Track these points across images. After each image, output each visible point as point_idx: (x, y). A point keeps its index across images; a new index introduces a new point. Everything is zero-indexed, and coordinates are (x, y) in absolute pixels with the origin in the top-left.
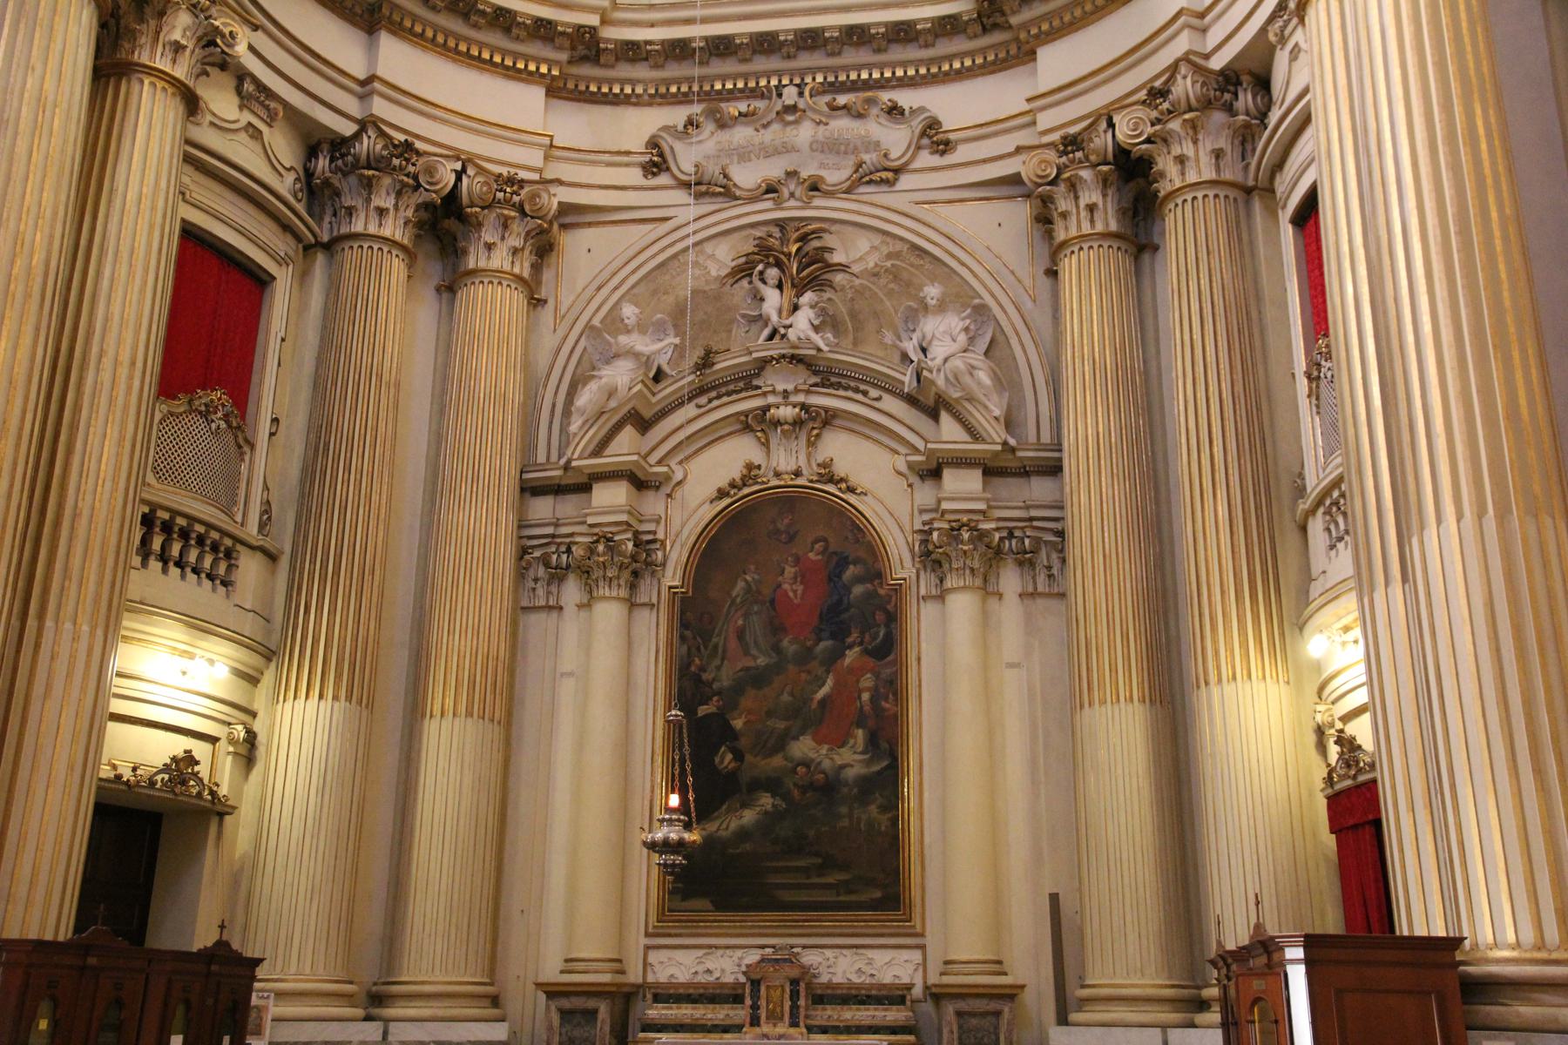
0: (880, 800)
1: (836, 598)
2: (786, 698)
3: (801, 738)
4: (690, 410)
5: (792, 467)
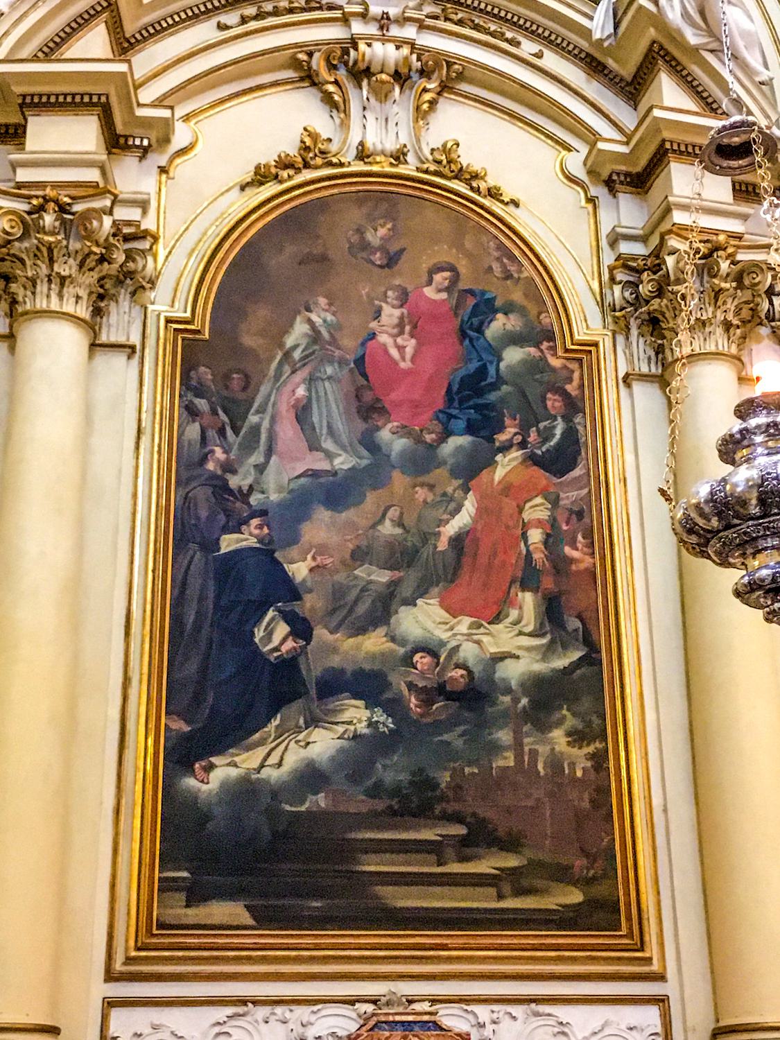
0: (571, 722)
1: (473, 366)
2: (388, 529)
3: (419, 602)
4: (205, 32)
5: (391, 145)
